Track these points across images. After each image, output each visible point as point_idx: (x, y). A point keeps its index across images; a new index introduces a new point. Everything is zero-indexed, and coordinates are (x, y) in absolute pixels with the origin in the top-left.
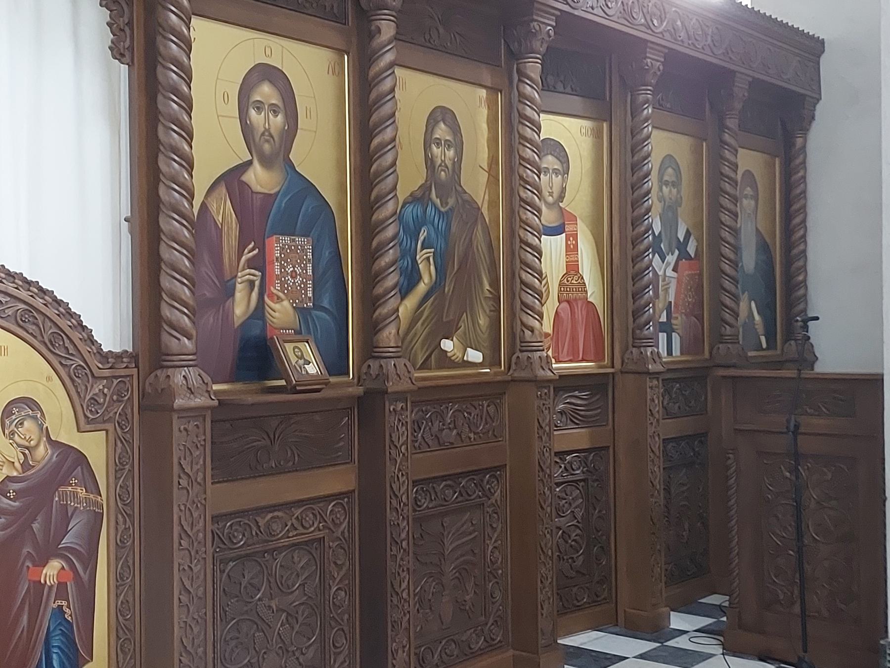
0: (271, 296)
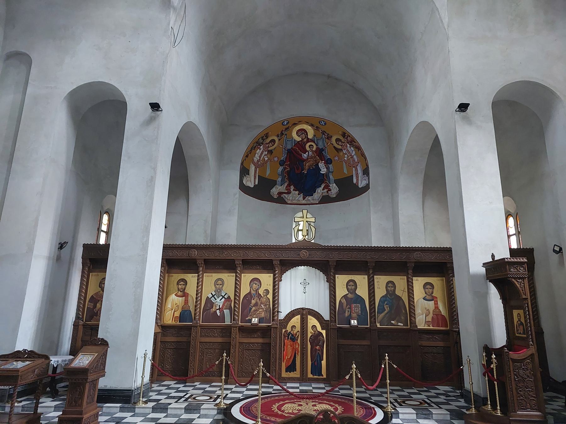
0: (352, 313)
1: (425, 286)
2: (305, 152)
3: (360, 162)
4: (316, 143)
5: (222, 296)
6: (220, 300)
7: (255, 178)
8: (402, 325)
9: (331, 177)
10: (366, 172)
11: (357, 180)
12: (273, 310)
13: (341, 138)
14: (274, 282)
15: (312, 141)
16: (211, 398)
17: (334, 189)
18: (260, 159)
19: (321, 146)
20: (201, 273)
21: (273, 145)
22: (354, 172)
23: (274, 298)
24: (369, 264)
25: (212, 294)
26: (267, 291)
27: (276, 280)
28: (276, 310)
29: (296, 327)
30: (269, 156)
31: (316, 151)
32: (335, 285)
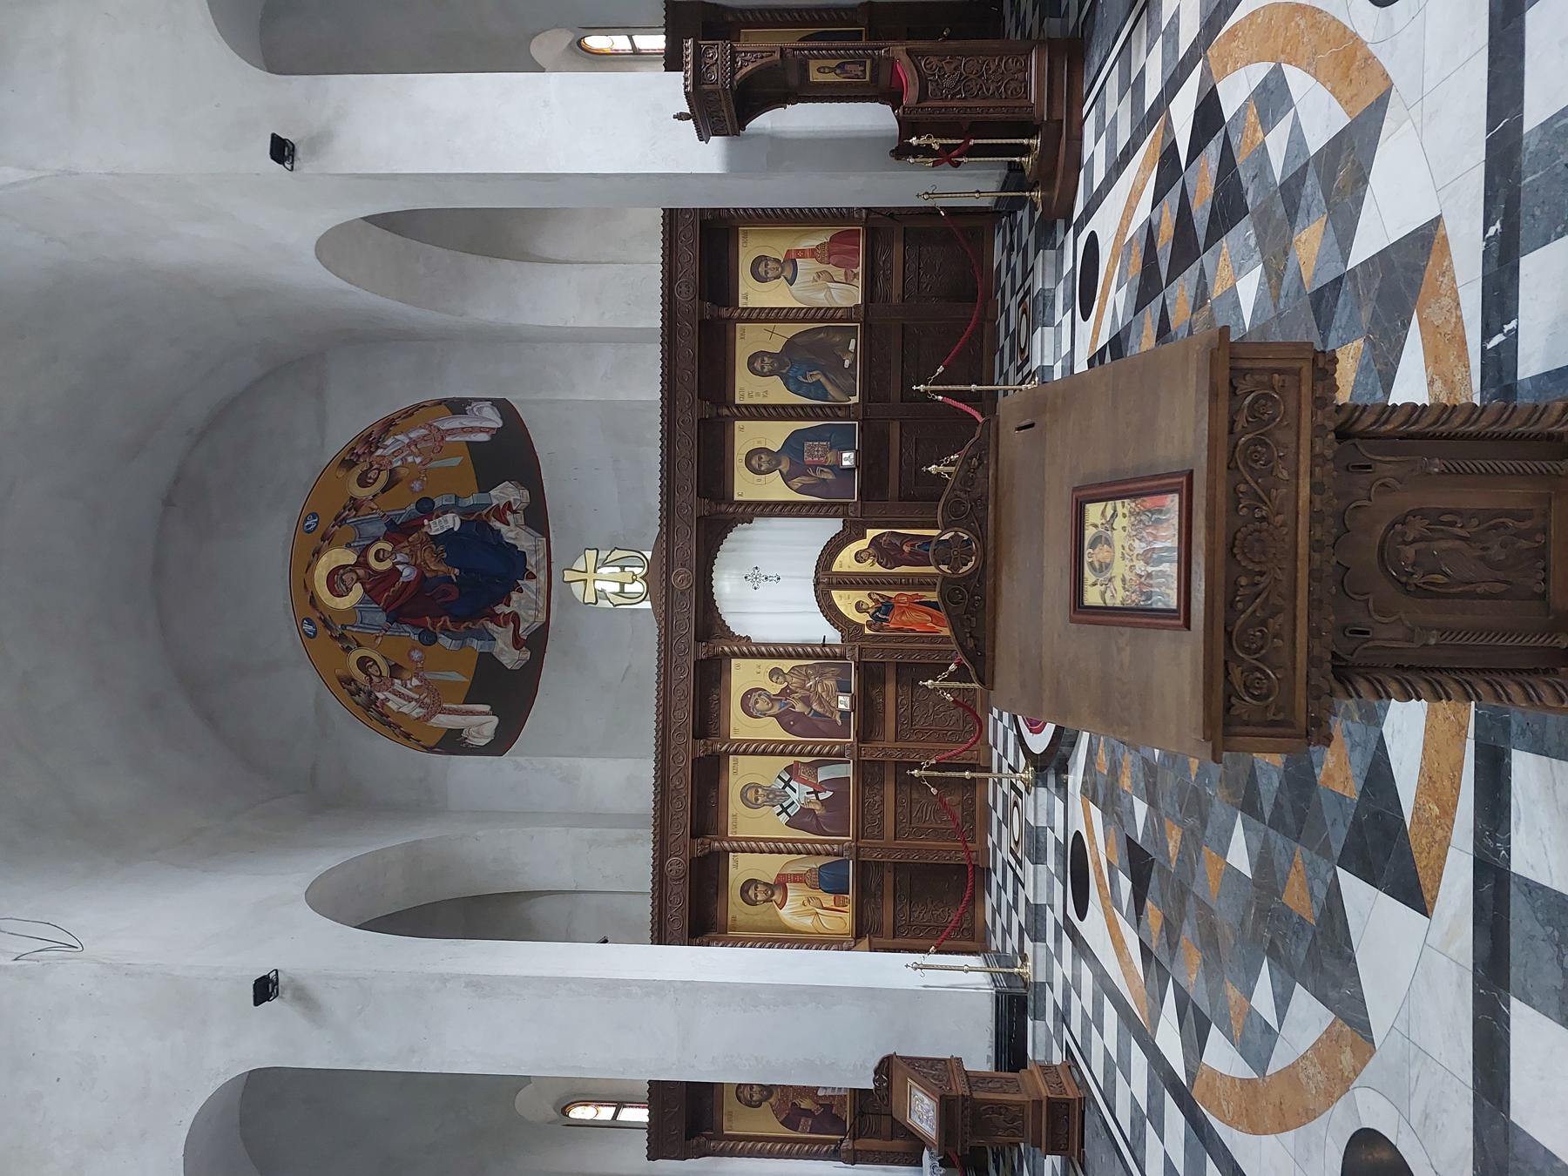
0: (826, 462)
1: (761, 279)
2: (394, 573)
3: (430, 422)
4: (370, 542)
5: (784, 788)
6: (795, 791)
7: (471, 712)
8: (853, 341)
9: (470, 501)
10: (458, 406)
11: (481, 430)
12: (818, 657)
13: (357, 471)
14: (752, 656)
15: (363, 553)
16: (1016, 804)
17: (506, 493)
18: (416, 700)
19: (380, 529)
20: (726, 845)
21: (375, 663)
22: (458, 439)
23: (790, 656)
24: (707, 417)
25: (778, 814)
26: (775, 673)
27: (747, 651)
28: (818, 650)
29: (859, 602)
30: (406, 675)
31: (395, 543)
32: (759, 503)
